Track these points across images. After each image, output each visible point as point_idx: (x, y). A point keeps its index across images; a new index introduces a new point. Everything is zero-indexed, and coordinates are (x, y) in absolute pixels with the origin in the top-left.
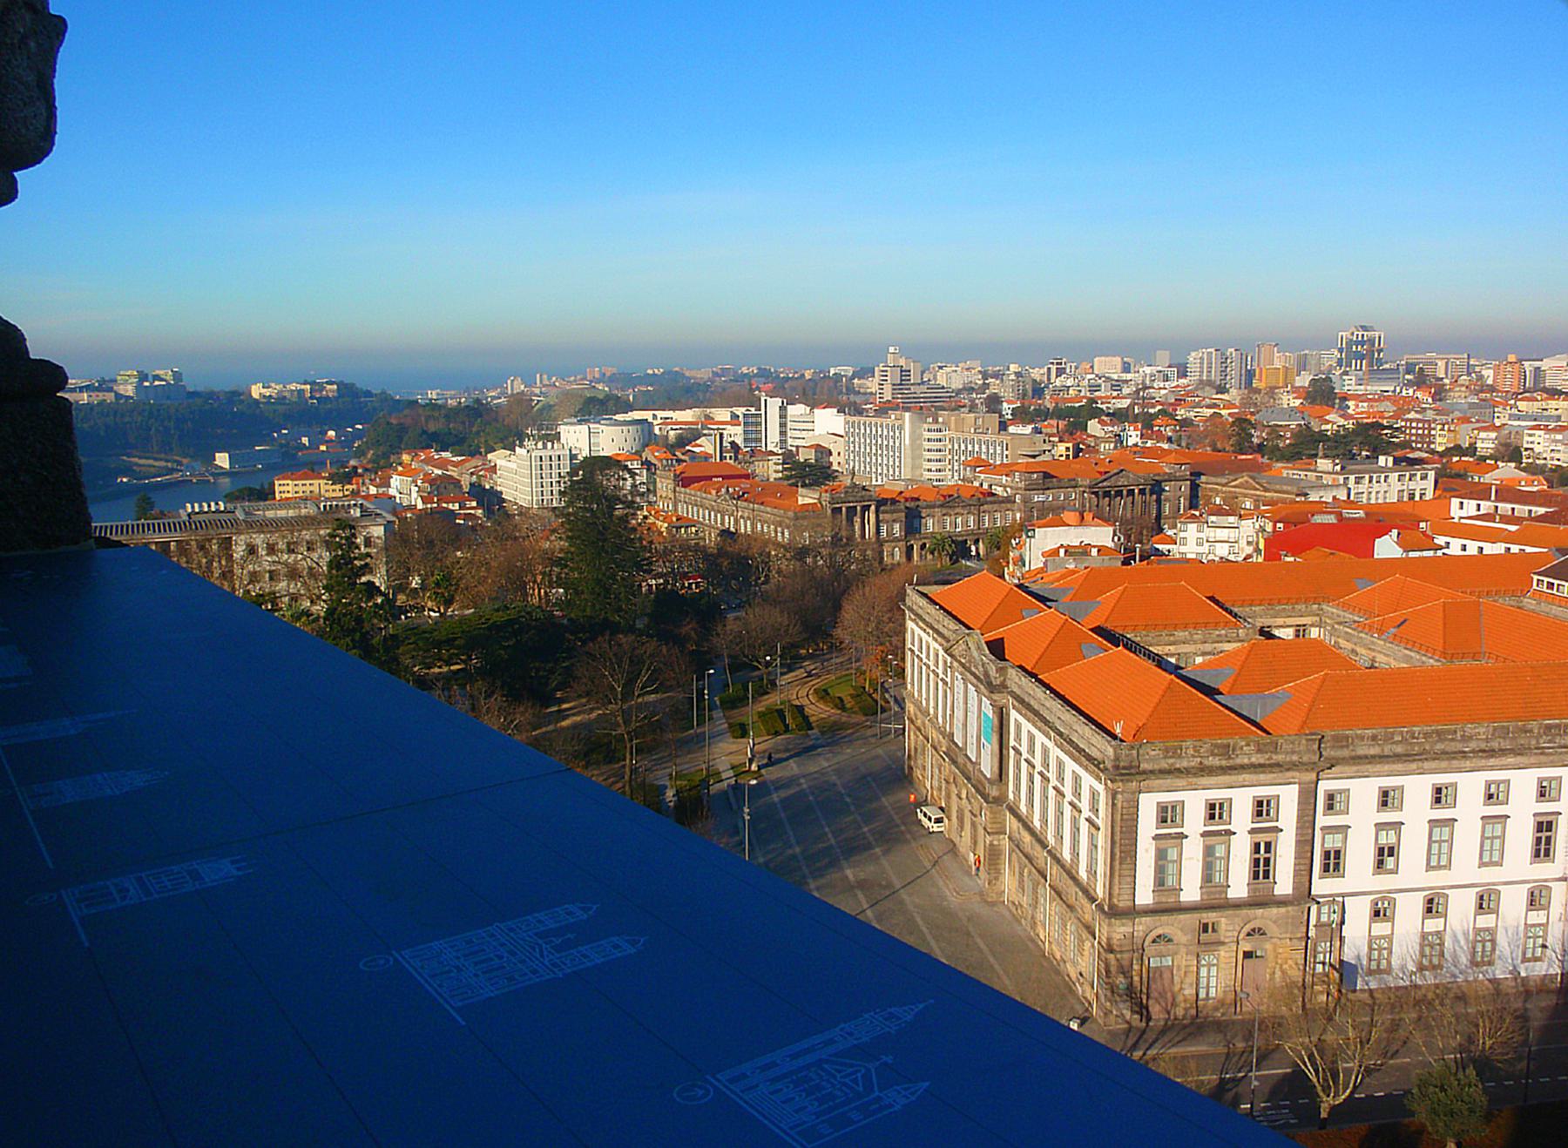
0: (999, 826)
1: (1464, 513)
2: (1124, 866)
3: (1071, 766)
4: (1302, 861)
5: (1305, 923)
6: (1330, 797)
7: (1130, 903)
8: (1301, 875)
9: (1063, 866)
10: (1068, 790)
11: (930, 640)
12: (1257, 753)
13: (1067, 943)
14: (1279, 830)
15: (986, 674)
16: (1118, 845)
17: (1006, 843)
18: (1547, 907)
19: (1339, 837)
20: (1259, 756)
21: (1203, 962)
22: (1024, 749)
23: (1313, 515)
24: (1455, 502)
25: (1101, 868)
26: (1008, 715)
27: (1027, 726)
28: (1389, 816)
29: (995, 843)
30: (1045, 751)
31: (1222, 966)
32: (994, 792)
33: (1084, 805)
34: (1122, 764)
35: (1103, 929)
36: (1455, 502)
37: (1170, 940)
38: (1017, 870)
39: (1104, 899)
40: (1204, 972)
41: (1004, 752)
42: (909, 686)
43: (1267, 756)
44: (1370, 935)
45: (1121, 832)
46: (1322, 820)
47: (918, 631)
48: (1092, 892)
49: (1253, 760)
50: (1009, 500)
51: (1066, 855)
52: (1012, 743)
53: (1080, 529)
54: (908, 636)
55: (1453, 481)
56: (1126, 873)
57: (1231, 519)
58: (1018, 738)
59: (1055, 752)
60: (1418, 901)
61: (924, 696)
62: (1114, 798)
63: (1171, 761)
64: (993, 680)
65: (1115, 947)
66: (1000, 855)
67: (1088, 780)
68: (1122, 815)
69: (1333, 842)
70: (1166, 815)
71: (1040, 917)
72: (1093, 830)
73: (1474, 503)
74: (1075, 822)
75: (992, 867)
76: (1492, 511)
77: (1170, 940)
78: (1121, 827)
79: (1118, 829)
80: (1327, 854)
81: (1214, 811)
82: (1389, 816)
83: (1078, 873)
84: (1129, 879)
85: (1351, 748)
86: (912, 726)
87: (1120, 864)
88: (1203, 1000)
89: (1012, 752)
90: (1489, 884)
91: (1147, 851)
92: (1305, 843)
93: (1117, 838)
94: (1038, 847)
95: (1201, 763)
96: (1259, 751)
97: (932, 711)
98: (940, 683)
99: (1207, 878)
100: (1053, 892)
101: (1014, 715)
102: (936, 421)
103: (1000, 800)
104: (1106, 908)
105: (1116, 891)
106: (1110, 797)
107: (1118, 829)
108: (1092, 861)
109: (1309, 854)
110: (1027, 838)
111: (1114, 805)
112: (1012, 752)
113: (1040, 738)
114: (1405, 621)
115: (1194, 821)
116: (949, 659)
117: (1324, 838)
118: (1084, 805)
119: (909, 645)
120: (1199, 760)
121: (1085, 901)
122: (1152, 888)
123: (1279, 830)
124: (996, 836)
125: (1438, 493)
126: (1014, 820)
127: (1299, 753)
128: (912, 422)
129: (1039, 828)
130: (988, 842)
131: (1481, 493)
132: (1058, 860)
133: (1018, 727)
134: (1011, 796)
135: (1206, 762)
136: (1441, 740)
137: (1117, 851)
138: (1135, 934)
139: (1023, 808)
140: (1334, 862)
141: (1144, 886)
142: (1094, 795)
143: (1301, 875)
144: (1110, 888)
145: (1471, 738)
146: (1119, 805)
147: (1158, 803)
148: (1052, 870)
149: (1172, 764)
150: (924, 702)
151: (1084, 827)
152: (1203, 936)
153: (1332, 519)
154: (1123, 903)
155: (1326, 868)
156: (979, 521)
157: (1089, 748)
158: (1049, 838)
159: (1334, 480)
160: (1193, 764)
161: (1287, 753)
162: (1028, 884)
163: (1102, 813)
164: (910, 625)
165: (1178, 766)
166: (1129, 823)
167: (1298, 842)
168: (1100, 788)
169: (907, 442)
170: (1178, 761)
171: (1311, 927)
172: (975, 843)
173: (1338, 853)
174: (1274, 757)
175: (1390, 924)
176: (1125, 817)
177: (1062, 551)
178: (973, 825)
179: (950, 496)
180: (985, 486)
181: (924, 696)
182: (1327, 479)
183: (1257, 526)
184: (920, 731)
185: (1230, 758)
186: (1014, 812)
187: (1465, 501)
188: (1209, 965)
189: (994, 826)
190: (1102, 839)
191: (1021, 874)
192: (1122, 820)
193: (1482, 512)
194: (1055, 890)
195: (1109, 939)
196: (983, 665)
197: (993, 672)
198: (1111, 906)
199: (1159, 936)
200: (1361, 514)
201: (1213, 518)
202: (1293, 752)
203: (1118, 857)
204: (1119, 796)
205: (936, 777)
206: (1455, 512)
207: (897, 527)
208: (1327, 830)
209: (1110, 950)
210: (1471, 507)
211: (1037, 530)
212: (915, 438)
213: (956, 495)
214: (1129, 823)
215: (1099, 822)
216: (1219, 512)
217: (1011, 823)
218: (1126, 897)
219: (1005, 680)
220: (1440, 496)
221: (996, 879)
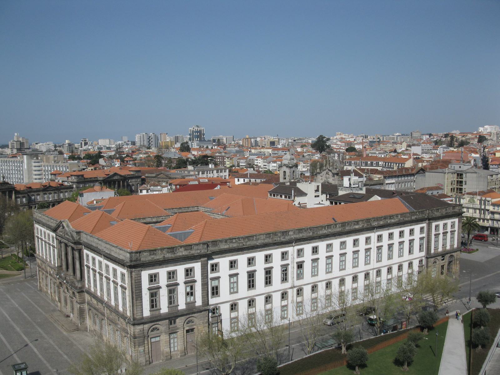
0: (82, 299)
1: (239, 183)
2: (138, 301)
3: (112, 265)
4: (204, 292)
5: (207, 316)
6: (212, 266)
7: (141, 316)
8: (205, 297)
9: (112, 308)
10: (111, 277)
11: (45, 230)
12: (185, 250)
13: (117, 339)
14: (195, 281)
15: (72, 237)
16: (134, 293)
17: (86, 307)
18: (287, 299)
19: (217, 281)
20: (185, 252)
21: (171, 337)
22: (91, 265)
23: (189, 182)
24: (236, 179)
25: (128, 304)
26: (83, 252)
27: (91, 255)
28: (233, 272)
29: (82, 307)
30: (100, 263)
31: (179, 337)
32: (79, 285)
33: (119, 281)
34: (133, 259)
35: (131, 329)
36: (236, 179)
37: (158, 330)
38: (92, 317)
39: (131, 316)
40: (172, 341)
41: (82, 268)
42: (37, 253)
43: (188, 252)
44: (230, 318)
45: (135, 288)
46: (211, 275)
47: (40, 227)
48: (125, 315)
49: (183, 253)
50: (71, 187)
51: (113, 303)
52: (85, 263)
53: (101, 193)
54: (36, 231)
55: (234, 173)
56: (139, 304)
57: (159, 187)
58: (88, 260)
59: (105, 262)
60: (245, 302)
61: (44, 255)
62: (131, 273)
63: (152, 256)
64: (75, 238)
65: (137, 335)
66: (84, 311)
67: (120, 270)
68: (135, 280)
69: (215, 283)
70: (153, 278)
71: (104, 333)
72: (123, 290)
73: (242, 179)
74: (116, 288)
75: (81, 317)
76: (249, 181)
77: (158, 330)
78: (135, 285)
79: (134, 287)
80: (213, 288)
81: (171, 275)
82: (233, 272)
83: (118, 309)
84: (140, 306)
85: (218, 246)
86: (40, 269)
87: (136, 301)
88: (173, 352)
89: (86, 268)
90: (268, 293)
91: (146, 294)
92: (205, 285)
93: (134, 290)
94: (100, 304)
95: (164, 257)
96: (186, 250)
97: (48, 260)
98: (51, 247)
99: (170, 303)
100: (108, 321)
101: (85, 252)
102: (37, 159)
103: (81, 291)
104: (132, 320)
105: (135, 312)
106: (130, 274)
107: (134, 287)
108: (124, 304)
109: (207, 289)
110: (94, 301)
111: (131, 277)
112: (86, 268)
113: (98, 258)
114: (229, 207)
115: (163, 281)
116: (54, 235)
117: (211, 282)
118: (119, 281)
119: (36, 234)
120: (163, 255)
121: (122, 320)
122: (149, 309)
123: (195, 281)
124: (82, 305)
125: (230, 177)
126: (88, 295)
127: (200, 249)
128: (27, 159)
129: (100, 295)
130: (78, 307)
131: (245, 176)
132: (108, 306)
133: (88, 256)
134: (87, 286)
135: (166, 256)
136: (249, 240)
137: (134, 296)
138: (145, 329)
139: (92, 290)
140: (216, 291)
141: (146, 309)
142: (123, 275)
143: (205, 297)
144: (133, 311)
145: (259, 239)
146: (134, 277)
147: (149, 274)
148: (106, 311)
149: (153, 258)
150: (45, 257)
151: (119, 289)
152: (171, 326)
153: (197, 183)
154: (138, 316)
155: (213, 294)
156: (59, 196)
157: (119, 256)
158: (105, 299)
159: (194, 173)
160: (161, 257)
161: (196, 250)
162: (98, 321)
163: (127, 282)
164: (36, 226)
165: (155, 258)
166: (138, 283)
167: (202, 284)
168: (125, 271)
169: (26, 167)
170: (155, 257)
171: (210, 317)
172: (73, 309)
173: (217, 288)
174: (191, 252)
175: (237, 312)
176: (136, 281)
177: (95, 202)
178: (72, 302)
179: (46, 186)
180: (60, 182)
181: (44, 255)
182: (192, 173)
183: (169, 187)
184: (44, 270)
185: (175, 253)
186: (89, 292)
187: (240, 179)
188: (174, 338)
189: (81, 299)
190: (128, 292)
191: (94, 317)
192: (135, 283)
193: (246, 182)
194: (110, 321)
195: (134, 332)
196: (70, 233)
197: (75, 235)
198: (134, 319)
199: (154, 329)
200: (207, 181)
201: (152, 187)
202: (198, 250)
203: (135, 298)
204: (133, 273)
205: (53, 288)
206: (237, 183)
207: (24, 200)
208: (213, 279)
209: (135, 337)
210: (242, 181)
211: (84, 194)
212: (29, 164)
213: (48, 186)
214: (138, 283)
215: (126, 286)
216: (155, 185)
217: (87, 297)
218: (139, 314)
219: (80, 238)
220: (231, 178)
221: (83, 322)
